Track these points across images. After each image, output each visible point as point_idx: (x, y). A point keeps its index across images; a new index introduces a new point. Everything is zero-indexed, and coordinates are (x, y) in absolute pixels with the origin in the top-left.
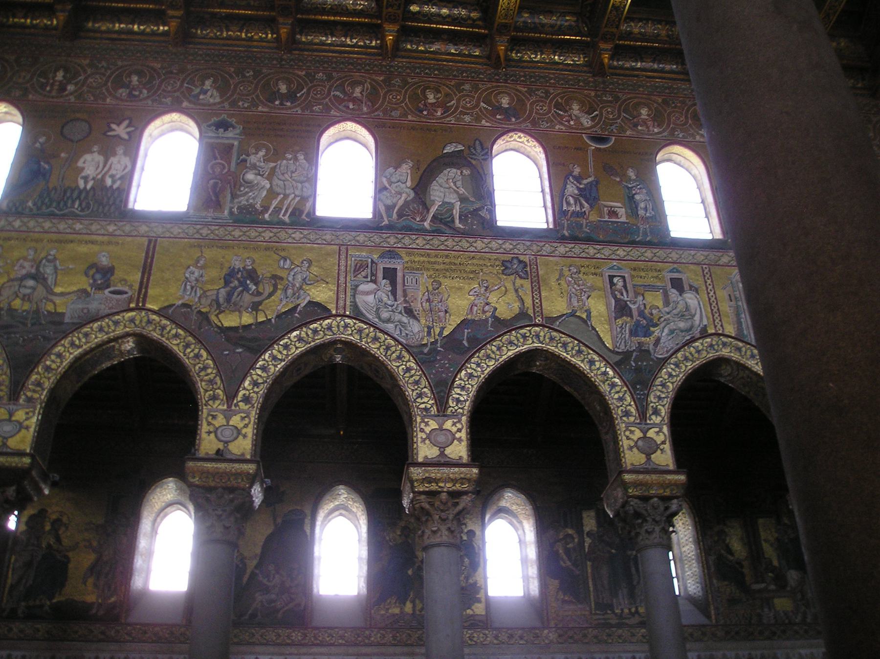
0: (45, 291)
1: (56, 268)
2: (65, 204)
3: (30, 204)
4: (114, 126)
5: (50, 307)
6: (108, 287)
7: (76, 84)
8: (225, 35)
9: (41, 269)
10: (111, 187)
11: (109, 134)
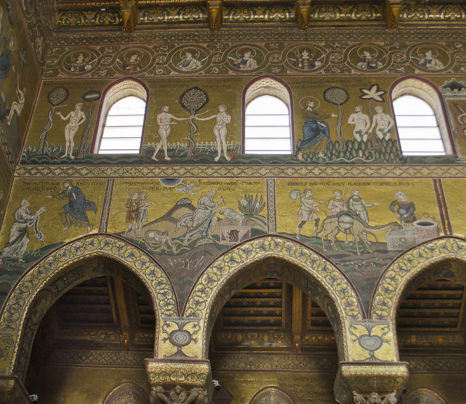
0: (361, 224)
1: (364, 206)
2: (351, 153)
3: (321, 155)
4: (366, 91)
5: (373, 239)
6: (415, 219)
7: (321, 61)
8: (426, 16)
9: (351, 207)
10: (384, 138)
11: (364, 97)
